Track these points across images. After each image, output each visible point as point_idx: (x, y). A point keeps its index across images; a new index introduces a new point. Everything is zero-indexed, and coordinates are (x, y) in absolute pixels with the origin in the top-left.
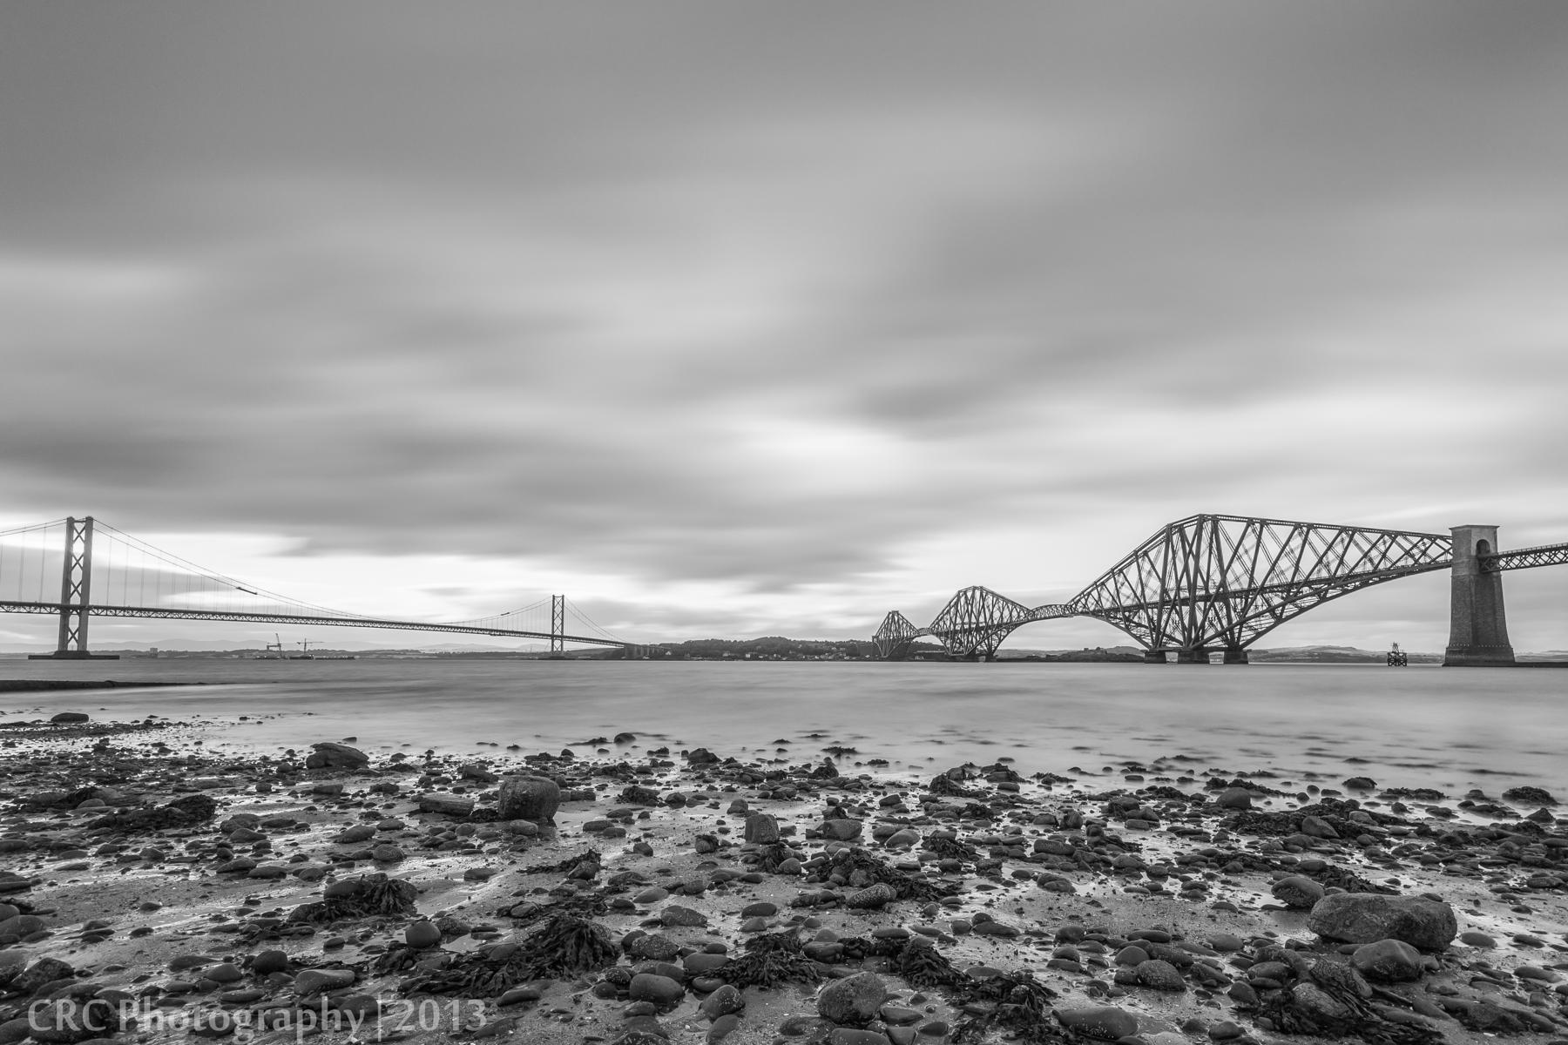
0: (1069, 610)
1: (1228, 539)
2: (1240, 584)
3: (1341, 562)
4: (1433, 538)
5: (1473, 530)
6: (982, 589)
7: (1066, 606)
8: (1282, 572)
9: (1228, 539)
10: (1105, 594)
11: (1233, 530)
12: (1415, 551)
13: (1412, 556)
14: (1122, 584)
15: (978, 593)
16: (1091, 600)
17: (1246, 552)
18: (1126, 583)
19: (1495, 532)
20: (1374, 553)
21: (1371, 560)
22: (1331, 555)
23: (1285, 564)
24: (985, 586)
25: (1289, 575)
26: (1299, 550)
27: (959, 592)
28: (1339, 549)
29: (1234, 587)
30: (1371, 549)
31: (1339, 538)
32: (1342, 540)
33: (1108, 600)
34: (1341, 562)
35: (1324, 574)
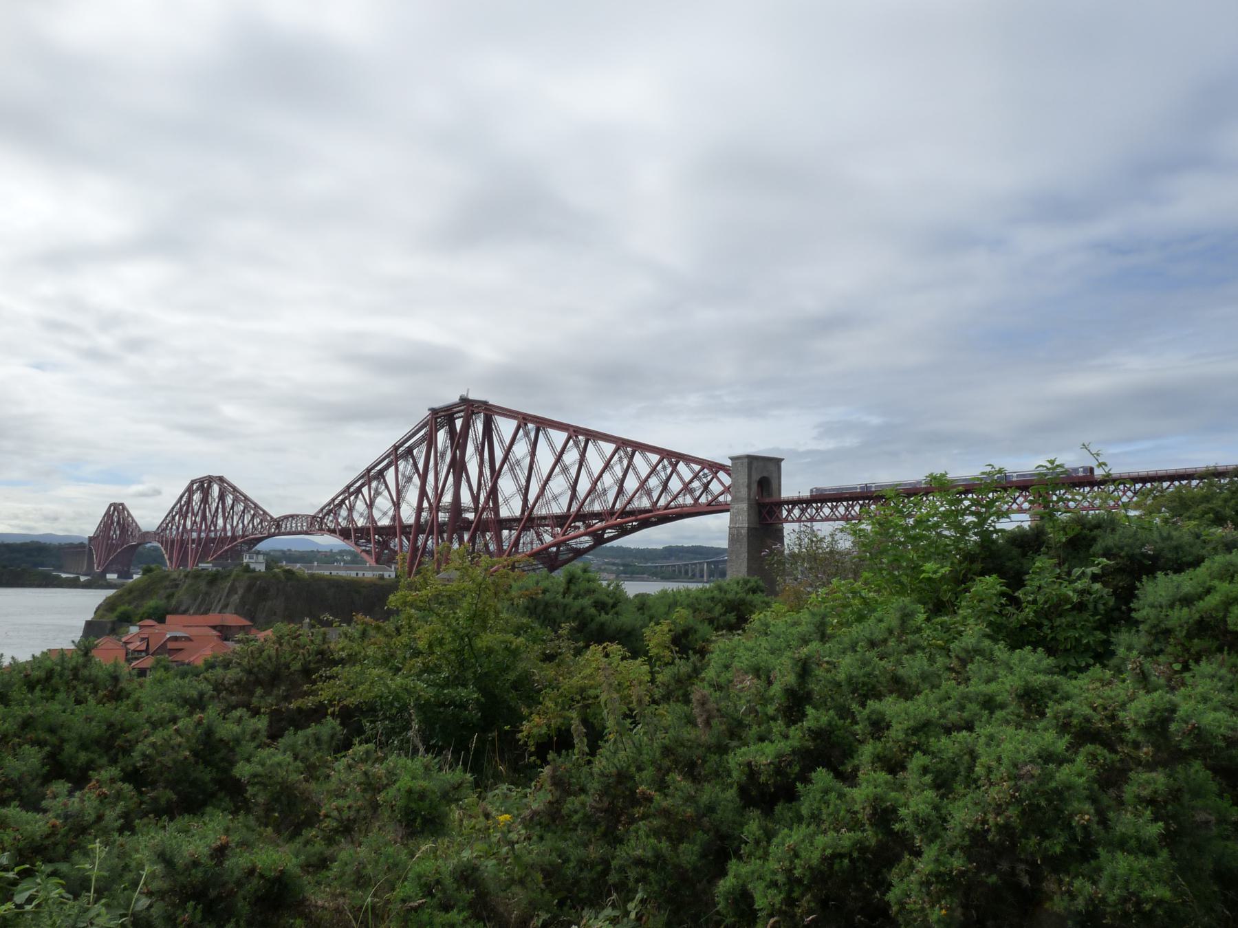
1: (501, 441)
2: (510, 509)
3: (621, 491)
4: (715, 468)
6: (221, 480)
8: (555, 498)
9: (501, 441)
11: (505, 427)
12: (696, 484)
13: (691, 491)
15: (215, 490)
17: (518, 462)
18: (386, 493)
20: (654, 482)
21: (649, 493)
22: (608, 480)
23: (559, 485)
24: (229, 477)
25: (564, 501)
26: (577, 466)
27: (193, 482)
28: (618, 470)
29: (504, 513)
30: (648, 477)
31: (616, 456)
32: (620, 460)
34: (621, 491)
35: (597, 507)
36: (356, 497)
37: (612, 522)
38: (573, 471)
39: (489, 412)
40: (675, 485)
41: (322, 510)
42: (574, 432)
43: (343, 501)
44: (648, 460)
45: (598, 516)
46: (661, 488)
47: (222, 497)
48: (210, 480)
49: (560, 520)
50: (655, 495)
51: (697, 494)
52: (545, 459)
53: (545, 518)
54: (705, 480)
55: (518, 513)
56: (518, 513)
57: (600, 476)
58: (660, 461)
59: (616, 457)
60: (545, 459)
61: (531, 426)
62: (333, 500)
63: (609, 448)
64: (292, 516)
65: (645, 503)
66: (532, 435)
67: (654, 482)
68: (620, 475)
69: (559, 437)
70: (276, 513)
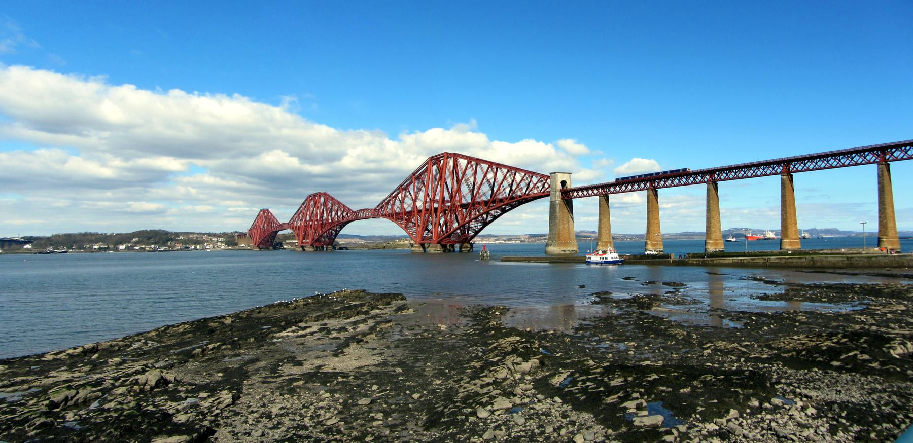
0: (377, 213)
2: (466, 200)
5: (560, 175)
6: (325, 194)
7: (374, 210)
8: (484, 194)
9: (461, 170)
10: (398, 203)
11: (463, 163)
12: (539, 184)
14: (407, 196)
15: (322, 199)
16: (389, 207)
17: (468, 179)
18: (409, 196)
19: (570, 177)
22: (505, 184)
23: (486, 188)
32: (510, 176)
33: (398, 207)
34: (511, 189)
35: (500, 196)
36: (396, 199)
37: (506, 202)
38: (492, 181)
39: (456, 156)
40: (531, 185)
41: (379, 206)
42: (491, 164)
43: (389, 201)
44: (521, 175)
45: (501, 200)
46: (526, 187)
47: (325, 203)
48: (320, 194)
49: (486, 203)
50: (524, 190)
51: (540, 188)
52: (480, 177)
53: (479, 203)
54: (543, 183)
55: (469, 201)
56: (469, 201)
57: (502, 183)
58: (525, 175)
59: (508, 175)
60: (480, 177)
61: (473, 162)
62: (384, 200)
63: (505, 171)
64: (364, 210)
65: (519, 193)
66: (474, 167)
67: (523, 184)
68: (511, 182)
69: (485, 166)
70: (355, 208)
